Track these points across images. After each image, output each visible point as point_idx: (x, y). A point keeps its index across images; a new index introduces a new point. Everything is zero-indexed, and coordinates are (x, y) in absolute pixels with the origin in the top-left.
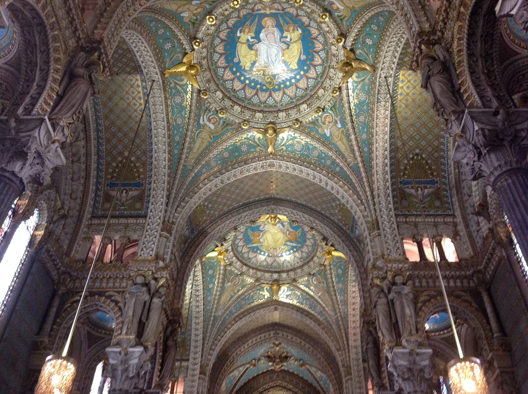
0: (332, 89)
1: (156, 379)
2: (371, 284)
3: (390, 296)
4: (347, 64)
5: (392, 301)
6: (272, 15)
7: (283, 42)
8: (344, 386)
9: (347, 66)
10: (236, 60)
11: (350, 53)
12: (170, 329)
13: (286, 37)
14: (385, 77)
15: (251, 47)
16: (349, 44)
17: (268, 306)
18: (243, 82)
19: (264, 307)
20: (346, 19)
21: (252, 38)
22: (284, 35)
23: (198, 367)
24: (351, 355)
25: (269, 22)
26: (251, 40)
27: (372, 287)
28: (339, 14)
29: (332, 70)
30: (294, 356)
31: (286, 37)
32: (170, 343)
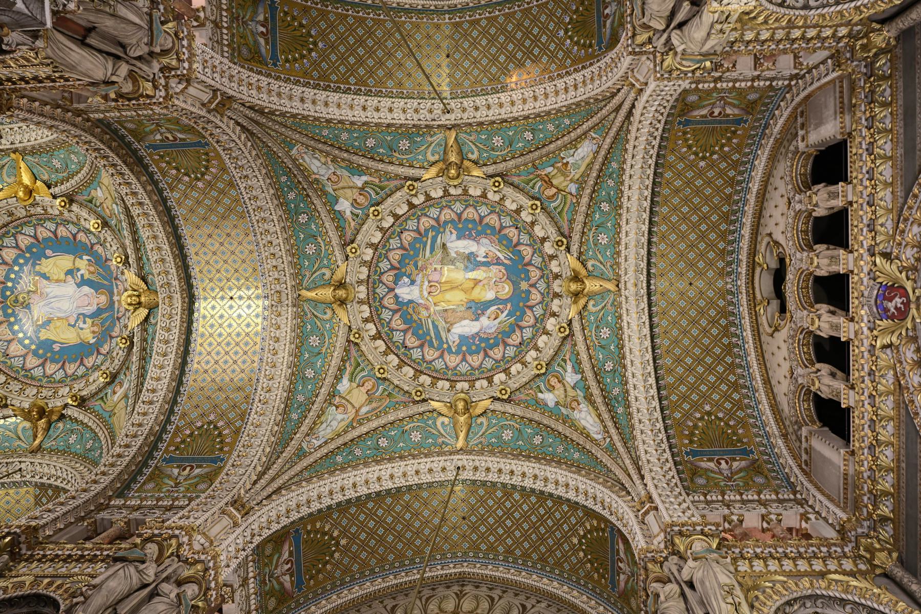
0: (6, 394)
4: (42, 413)
6: (112, 303)
7: (78, 319)
9: (38, 413)
10: (49, 252)
11: (59, 414)
13: (85, 322)
14: (20, 470)
15: (70, 272)
16: (69, 412)
18: (15, 262)
20: (103, 404)
21: (82, 275)
22: (87, 319)
25: (103, 299)
26: (79, 274)
28: (109, 395)
29: (35, 391)
31: (85, 322)
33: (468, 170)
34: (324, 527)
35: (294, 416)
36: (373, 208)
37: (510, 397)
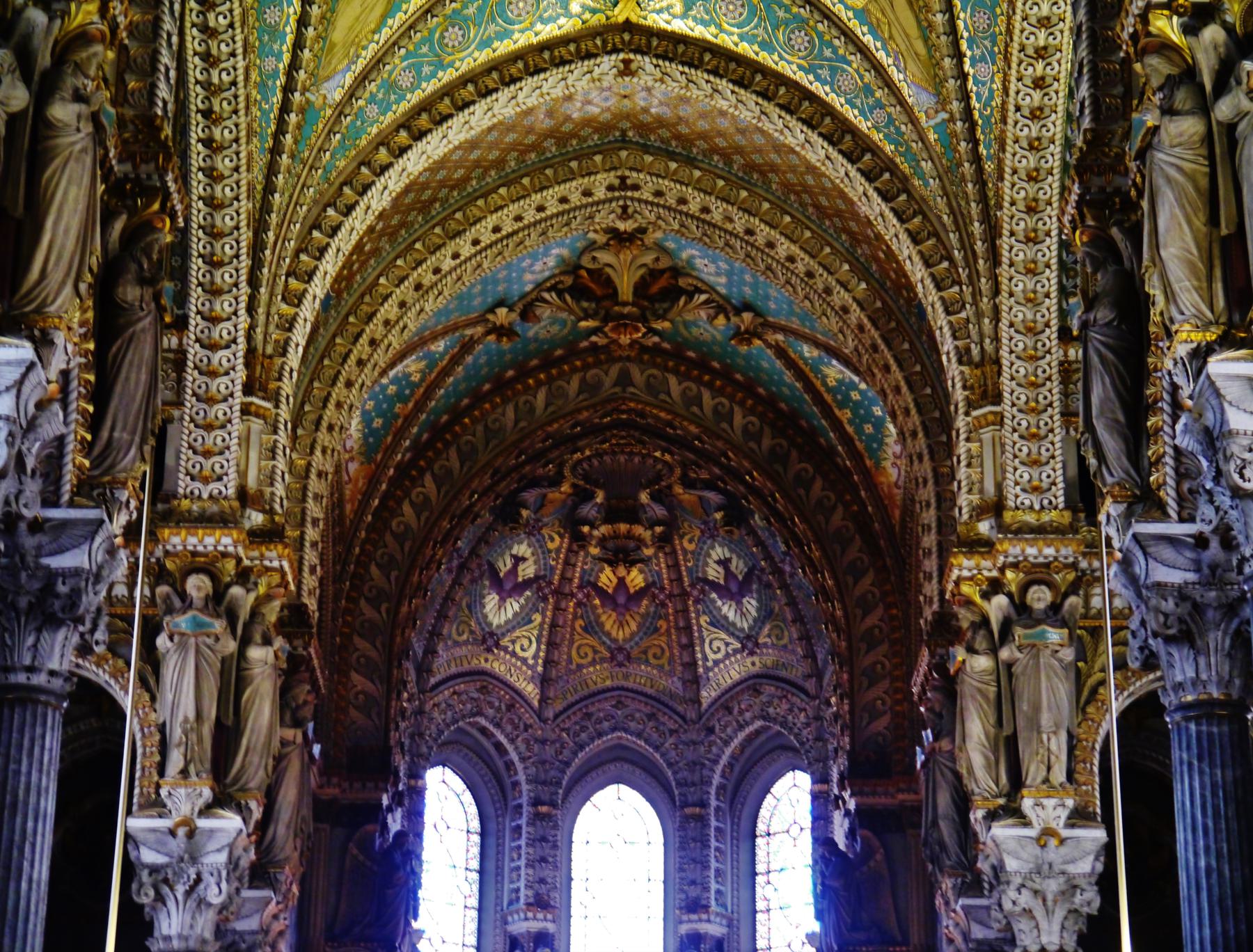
1: (74, 461)
2: (1134, 37)
3: (1224, 110)
5: (1230, 128)
8: (962, 448)
12: (118, 226)
17: (589, 56)
19: (563, 62)
23: (232, 359)
24: (1004, 301)
27: (1141, 54)
30: (711, 289)
32: (131, 293)
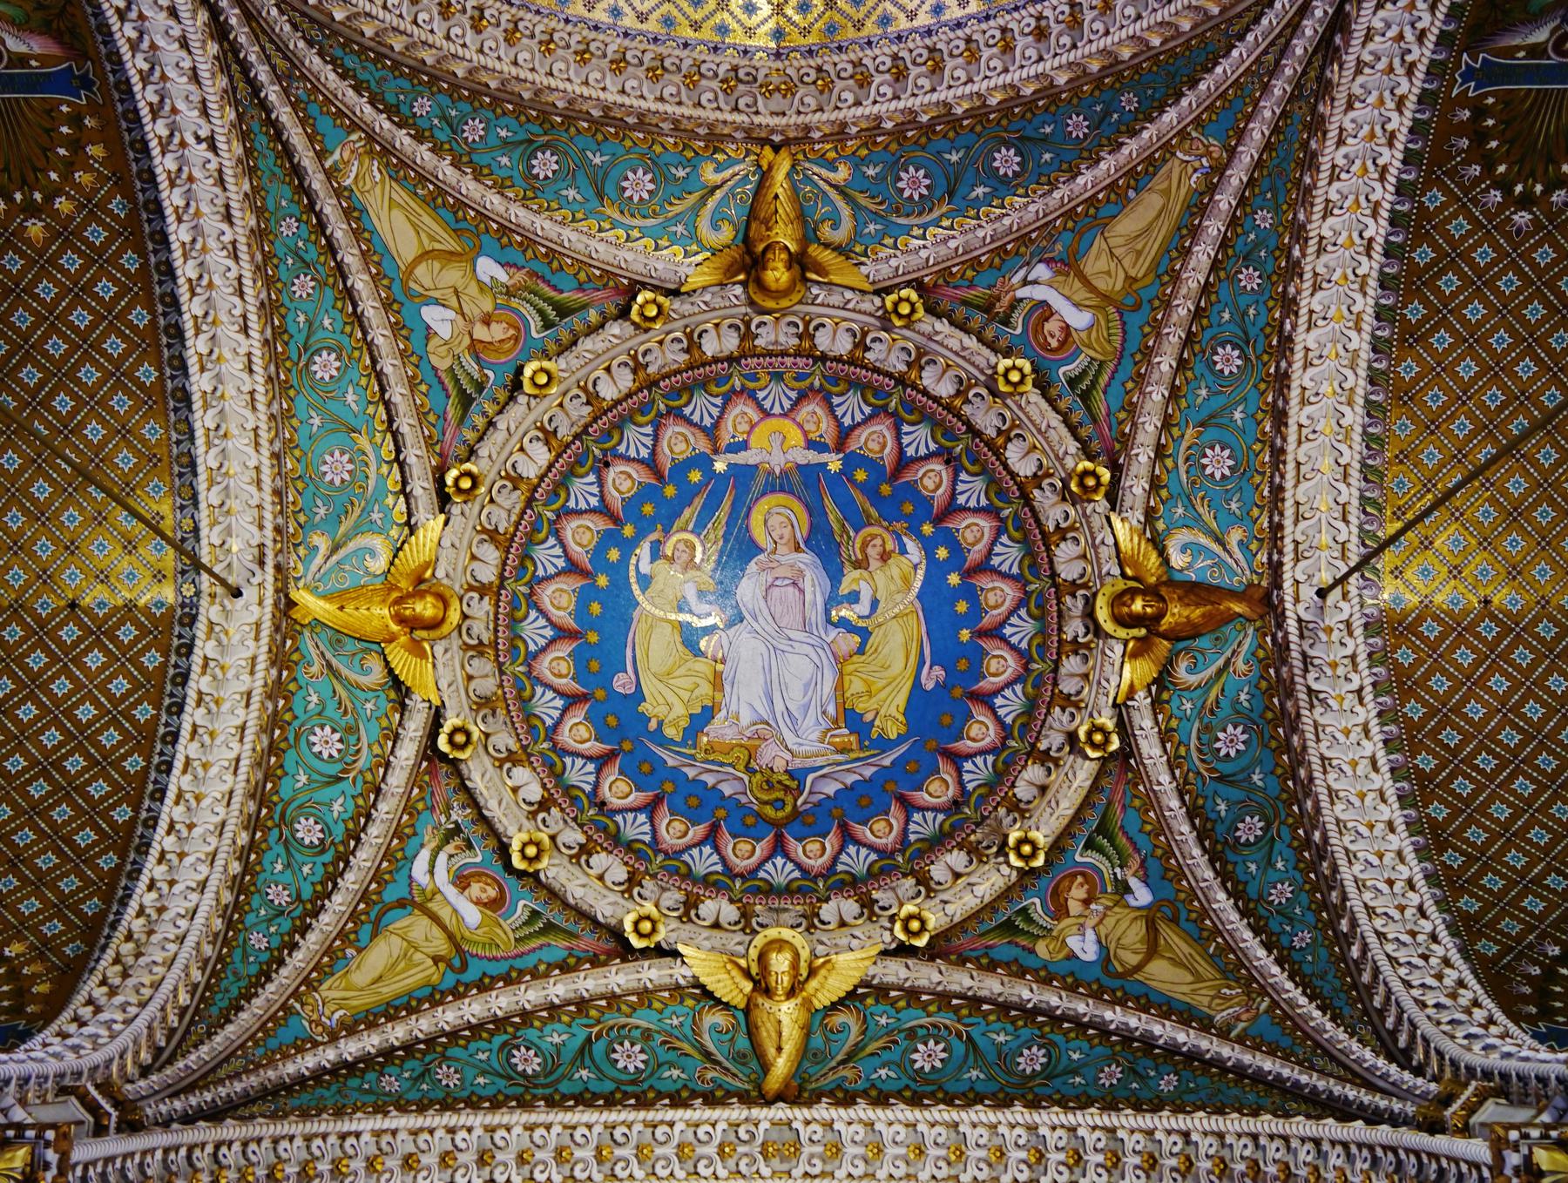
33: (1142, 649)
34: (88, 169)
35: (423, 106)
36: (1027, 368)
37: (443, 757)
